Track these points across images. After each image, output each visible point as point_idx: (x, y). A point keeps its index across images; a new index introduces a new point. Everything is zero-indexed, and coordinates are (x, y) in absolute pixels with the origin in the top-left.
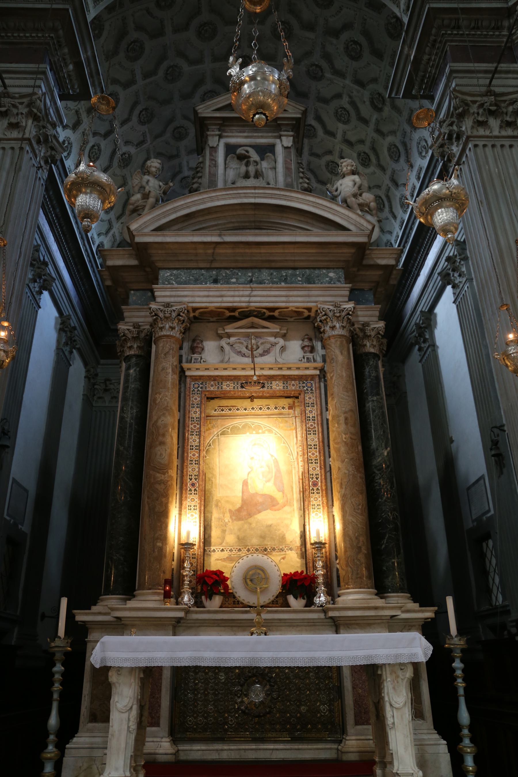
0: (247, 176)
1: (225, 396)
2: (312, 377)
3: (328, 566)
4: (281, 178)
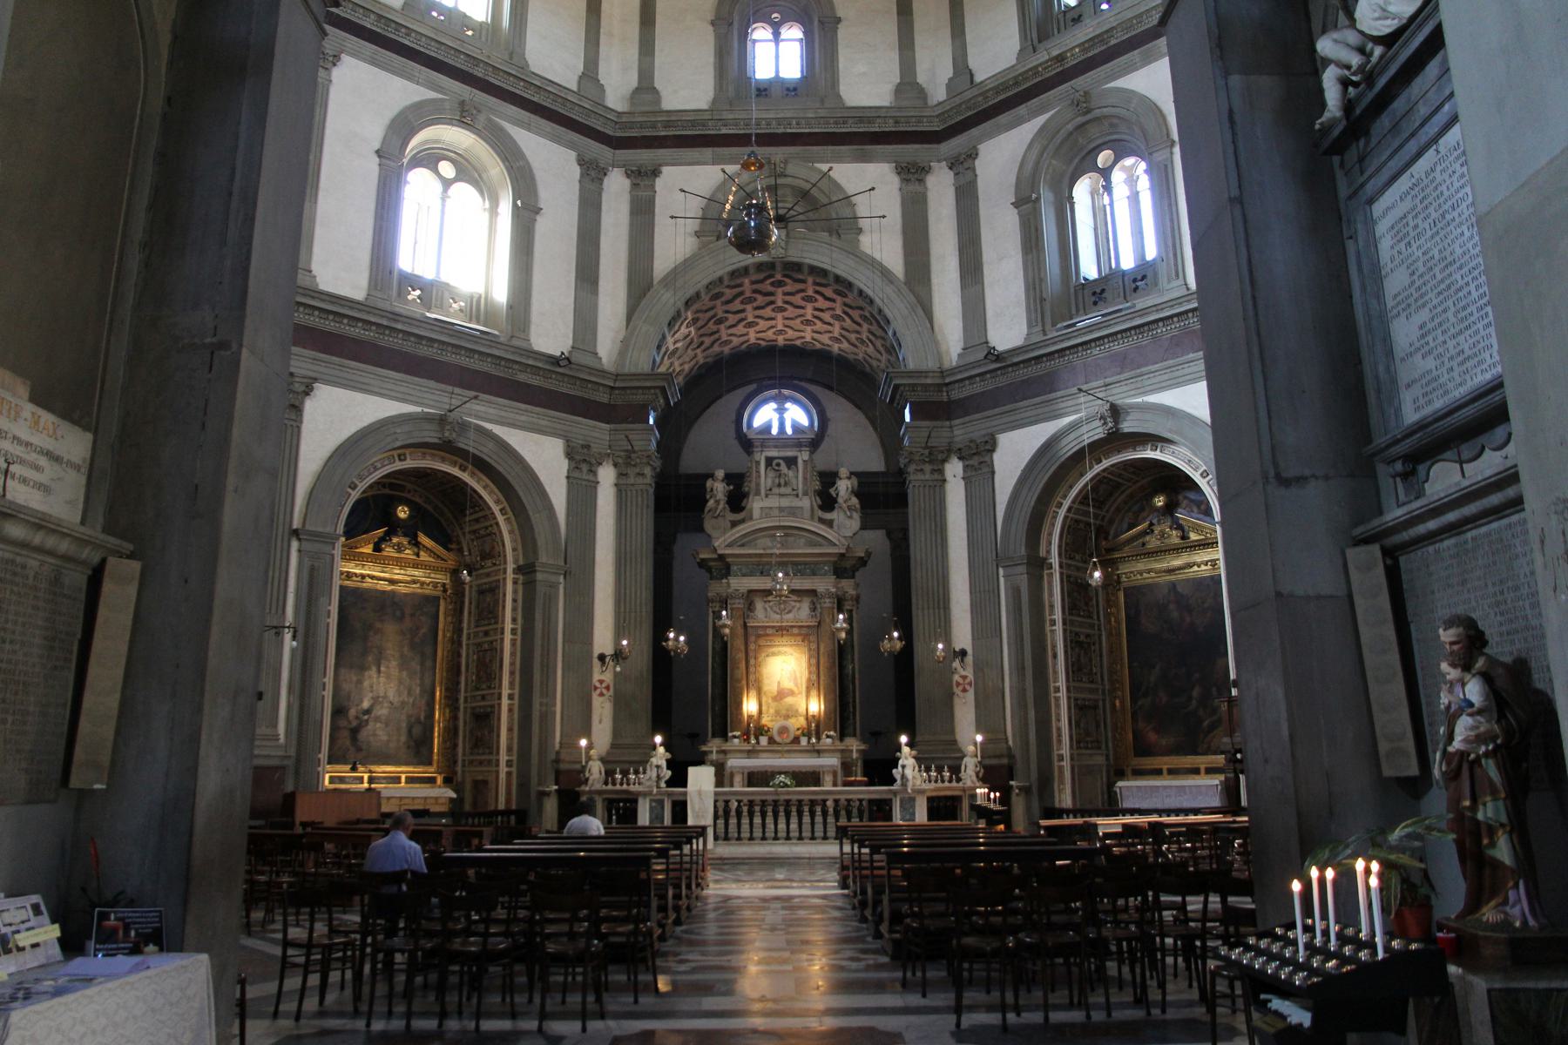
0: (779, 485)
1: (768, 635)
2: (814, 626)
3: (818, 726)
4: (800, 486)
